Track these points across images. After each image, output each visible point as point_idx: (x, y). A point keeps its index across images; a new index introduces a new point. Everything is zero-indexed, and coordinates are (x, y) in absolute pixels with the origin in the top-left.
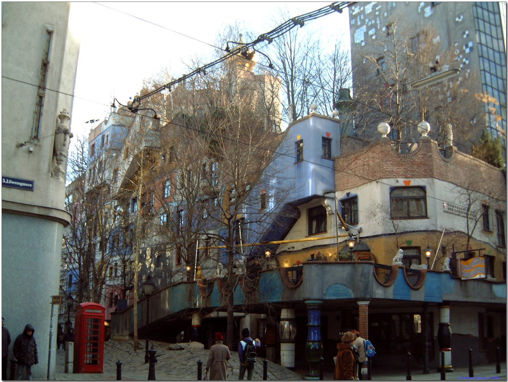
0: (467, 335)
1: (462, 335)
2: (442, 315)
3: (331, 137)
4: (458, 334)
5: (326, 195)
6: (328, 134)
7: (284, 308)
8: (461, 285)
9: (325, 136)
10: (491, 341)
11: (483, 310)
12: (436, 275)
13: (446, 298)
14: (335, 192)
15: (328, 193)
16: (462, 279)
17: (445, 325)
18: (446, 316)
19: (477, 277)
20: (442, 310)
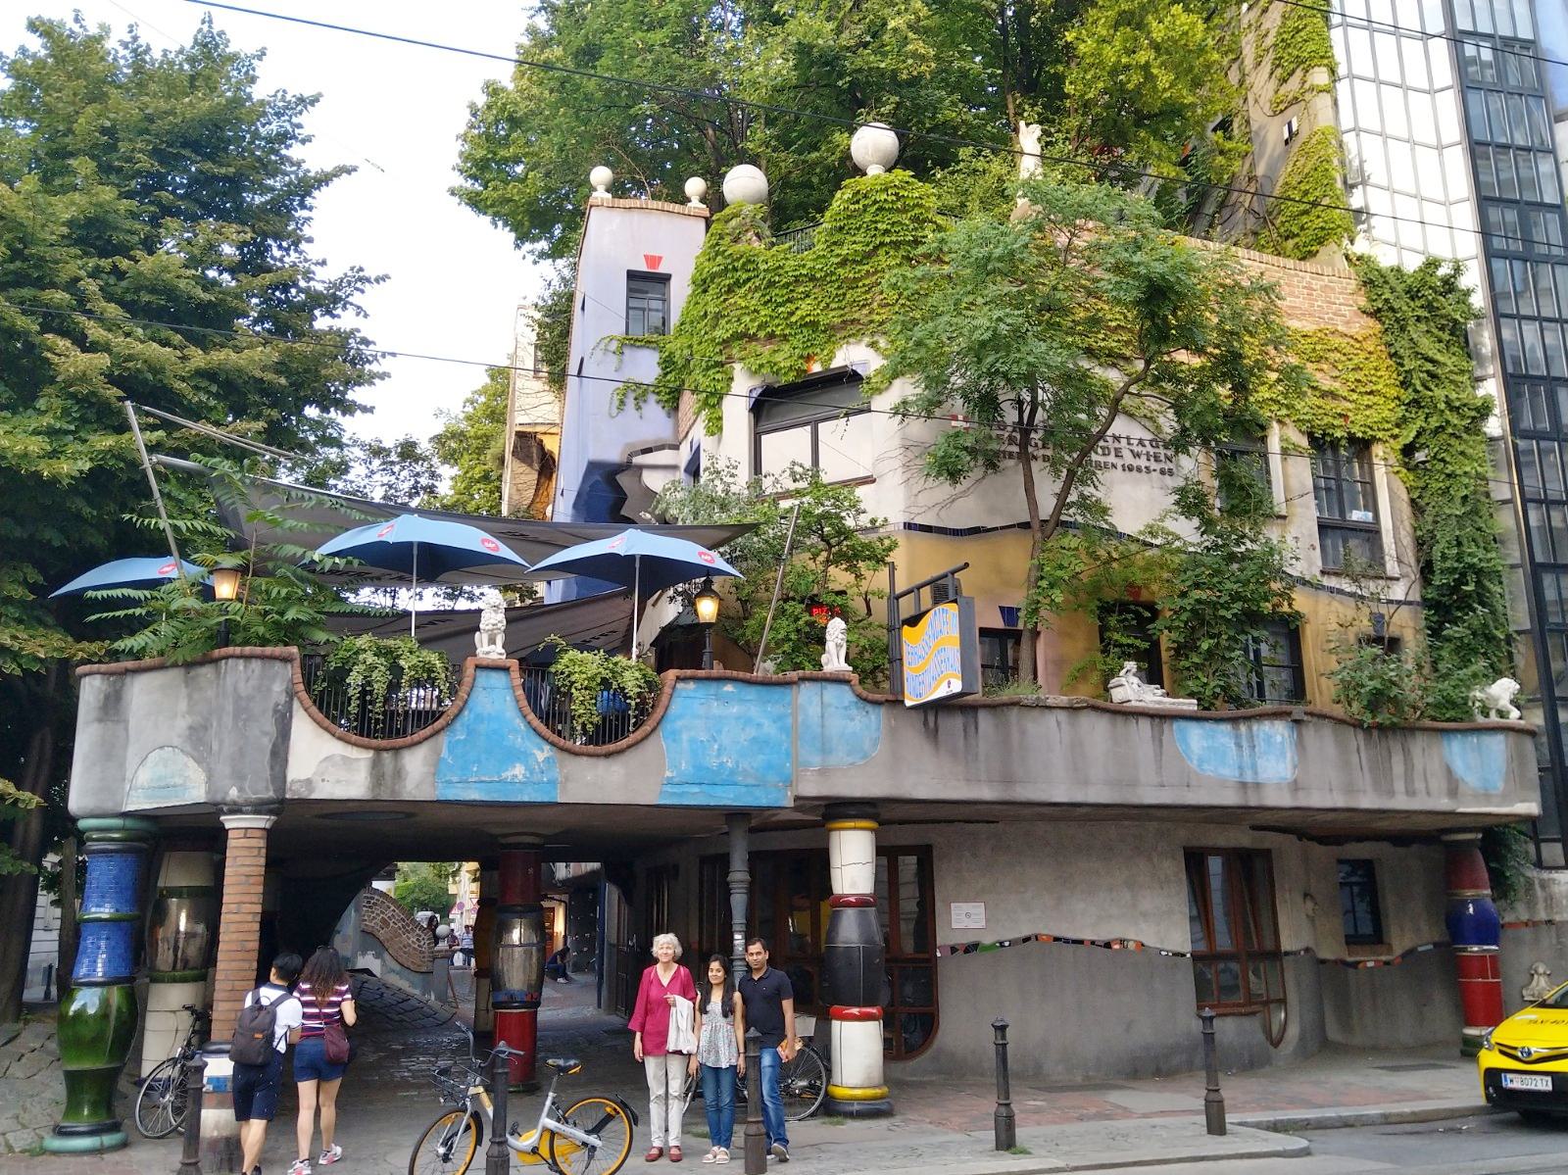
0: (1108, 945)
1: (1081, 942)
2: (836, 860)
3: (662, 269)
4: (1056, 939)
5: (638, 460)
6: (653, 260)
7: (175, 848)
8: (933, 734)
9: (642, 267)
10: (1370, 964)
11: (1244, 839)
12: (752, 693)
13: (811, 788)
14: (676, 447)
15: (648, 450)
16: (908, 703)
17: (849, 905)
18: (853, 862)
19: (941, 692)
20: (835, 836)
